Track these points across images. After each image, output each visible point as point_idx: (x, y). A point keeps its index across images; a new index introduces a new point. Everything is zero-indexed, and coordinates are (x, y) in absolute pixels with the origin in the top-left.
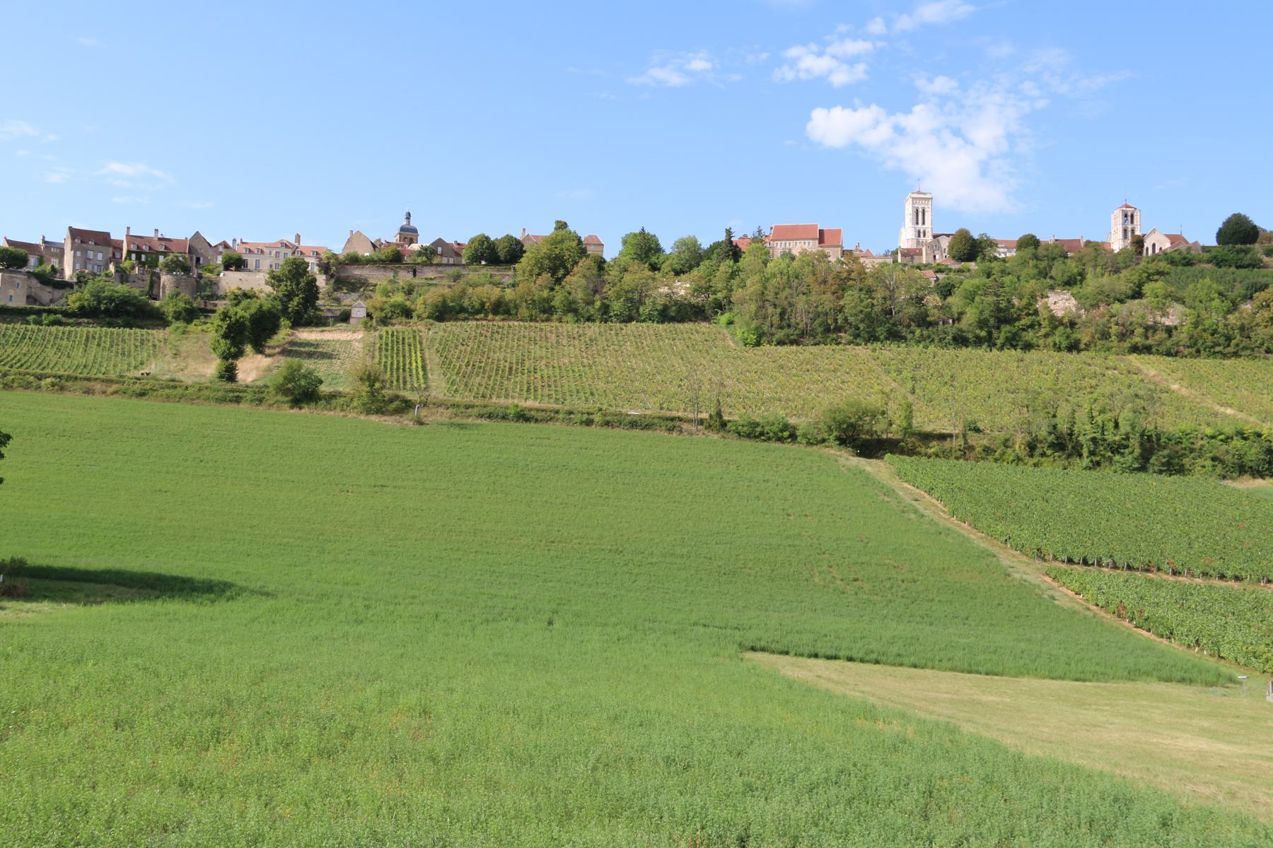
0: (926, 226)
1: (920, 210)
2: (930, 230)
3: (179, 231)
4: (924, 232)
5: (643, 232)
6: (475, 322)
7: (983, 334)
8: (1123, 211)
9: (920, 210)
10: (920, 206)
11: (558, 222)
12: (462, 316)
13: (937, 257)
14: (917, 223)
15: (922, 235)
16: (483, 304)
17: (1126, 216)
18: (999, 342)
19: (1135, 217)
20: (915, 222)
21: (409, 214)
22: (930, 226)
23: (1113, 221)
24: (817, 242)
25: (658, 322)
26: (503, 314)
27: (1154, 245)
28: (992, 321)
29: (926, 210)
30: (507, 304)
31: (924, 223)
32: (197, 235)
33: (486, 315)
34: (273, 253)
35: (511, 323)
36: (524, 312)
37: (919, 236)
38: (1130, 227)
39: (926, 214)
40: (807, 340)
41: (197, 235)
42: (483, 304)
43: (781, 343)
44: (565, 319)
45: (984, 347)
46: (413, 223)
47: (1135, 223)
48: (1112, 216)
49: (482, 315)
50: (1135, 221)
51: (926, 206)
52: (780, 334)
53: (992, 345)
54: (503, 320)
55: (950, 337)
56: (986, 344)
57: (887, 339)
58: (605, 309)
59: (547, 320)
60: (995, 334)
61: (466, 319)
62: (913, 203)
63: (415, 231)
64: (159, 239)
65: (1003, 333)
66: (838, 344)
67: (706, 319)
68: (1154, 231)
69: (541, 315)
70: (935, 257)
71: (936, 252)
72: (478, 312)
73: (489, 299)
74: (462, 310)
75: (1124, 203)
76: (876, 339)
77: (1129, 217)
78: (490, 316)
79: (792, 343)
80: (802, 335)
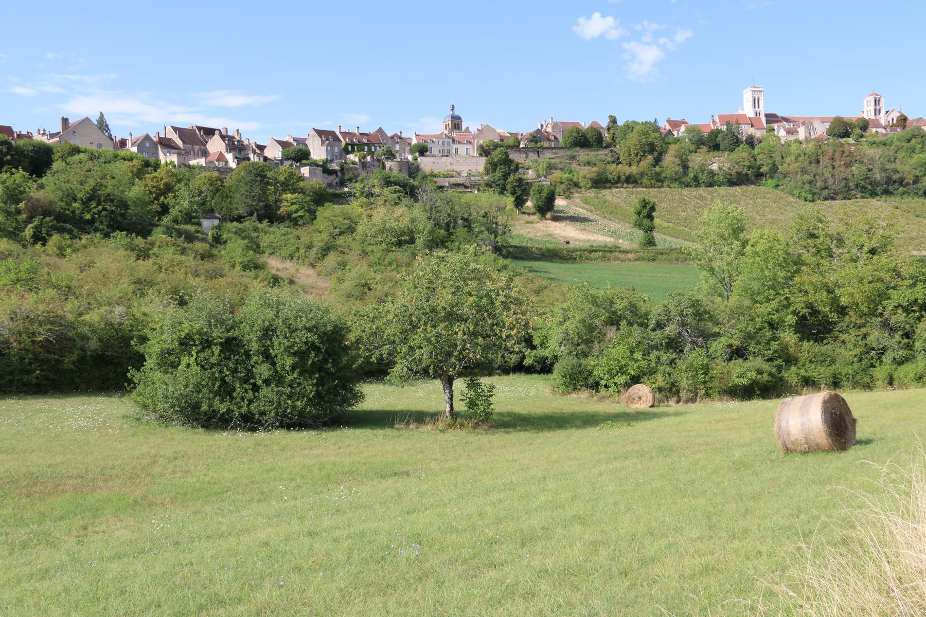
3: (371, 130)
6: (616, 190)
11: (611, 117)
12: (608, 185)
16: (619, 177)
21: (453, 106)
30: (634, 177)
32: (380, 130)
34: (441, 143)
35: (639, 189)
36: (645, 181)
40: (840, 196)
41: (380, 130)
42: (619, 177)
43: (826, 199)
44: (672, 185)
46: (457, 113)
52: (825, 192)
54: (633, 187)
55: (922, 192)
57: (882, 194)
58: (696, 178)
59: (662, 187)
61: (610, 188)
63: (459, 118)
64: (361, 134)
66: (856, 198)
67: (753, 183)
72: (617, 182)
73: (625, 173)
74: (607, 181)
76: (877, 195)
78: (625, 185)
79: (833, 199)
80: (836, 193)
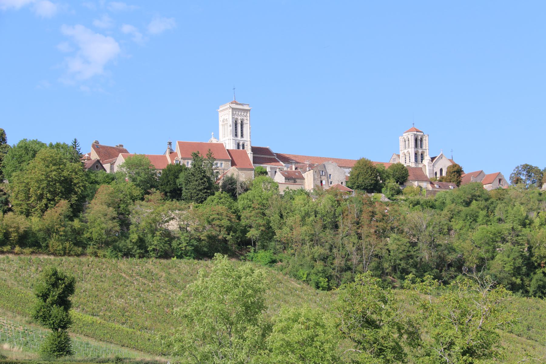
0: (244, 139)
1: (239, 122)
2: (249, 143)
4: (243, 145)
5: (57, 143)
7: (518, 281)
8: (415, 134)
9: (239, 122)
10: (239, 118)
13: (324, 182)
14: (236, 135)
15: (241, 148)
17: (416, 140)
18: (531, 290)
19: (424, 141)
20: (235, 133)
22: (249, 140)
23: (402, 144)
24: (230, 163)
25: (194, 258)
26: (30, 247)
27: (441, 170)
28: (524, 269)
29: (245, 122)
31: (242, 136)
33: (13, 248)
36: (54, 243)
37: (238, 148)
38: (420, 151)
39: (245, 126)
42: (7, 235)
45: (519, 293)
47: (424, 148)
48: (401, 139)
49: (9, 247)
50: (424, 145)
51: (245, 118)
53: (526, 293)
54: (32, 253)
56: (521, 291)
58: (141, 243)
60: (527, 283)
62: (233, 114)
65: (534, 281)
68: (441, 157)
69: (76, 248)
70: (321, 182)
71: (323, 177)
75: (412, 126)
77: (418, 142)
78: (17, 249)
